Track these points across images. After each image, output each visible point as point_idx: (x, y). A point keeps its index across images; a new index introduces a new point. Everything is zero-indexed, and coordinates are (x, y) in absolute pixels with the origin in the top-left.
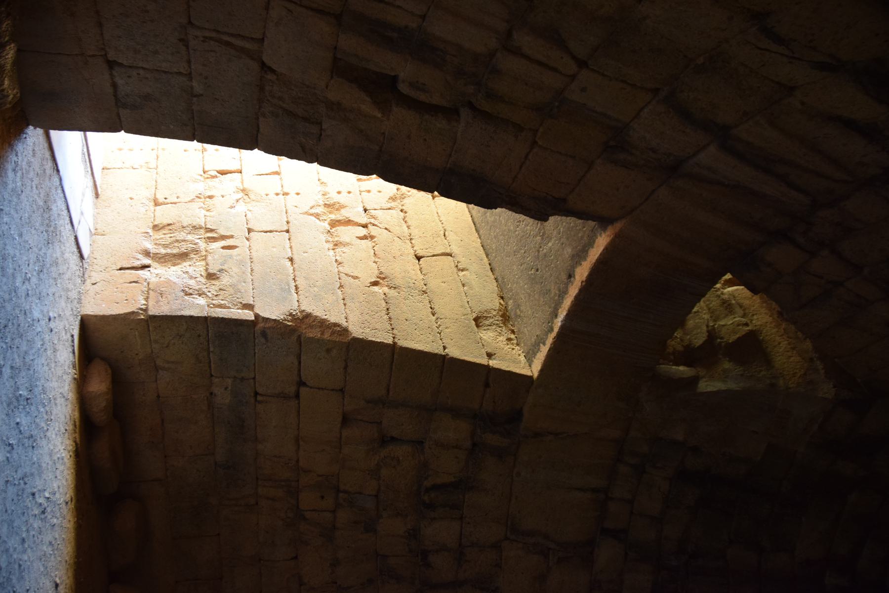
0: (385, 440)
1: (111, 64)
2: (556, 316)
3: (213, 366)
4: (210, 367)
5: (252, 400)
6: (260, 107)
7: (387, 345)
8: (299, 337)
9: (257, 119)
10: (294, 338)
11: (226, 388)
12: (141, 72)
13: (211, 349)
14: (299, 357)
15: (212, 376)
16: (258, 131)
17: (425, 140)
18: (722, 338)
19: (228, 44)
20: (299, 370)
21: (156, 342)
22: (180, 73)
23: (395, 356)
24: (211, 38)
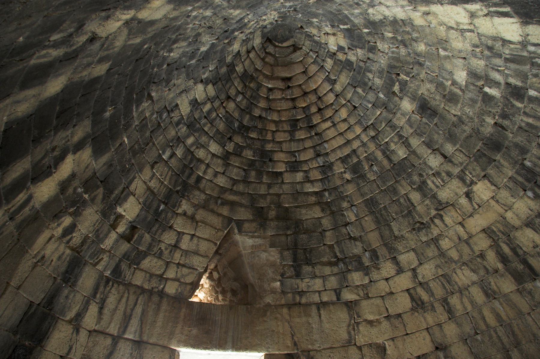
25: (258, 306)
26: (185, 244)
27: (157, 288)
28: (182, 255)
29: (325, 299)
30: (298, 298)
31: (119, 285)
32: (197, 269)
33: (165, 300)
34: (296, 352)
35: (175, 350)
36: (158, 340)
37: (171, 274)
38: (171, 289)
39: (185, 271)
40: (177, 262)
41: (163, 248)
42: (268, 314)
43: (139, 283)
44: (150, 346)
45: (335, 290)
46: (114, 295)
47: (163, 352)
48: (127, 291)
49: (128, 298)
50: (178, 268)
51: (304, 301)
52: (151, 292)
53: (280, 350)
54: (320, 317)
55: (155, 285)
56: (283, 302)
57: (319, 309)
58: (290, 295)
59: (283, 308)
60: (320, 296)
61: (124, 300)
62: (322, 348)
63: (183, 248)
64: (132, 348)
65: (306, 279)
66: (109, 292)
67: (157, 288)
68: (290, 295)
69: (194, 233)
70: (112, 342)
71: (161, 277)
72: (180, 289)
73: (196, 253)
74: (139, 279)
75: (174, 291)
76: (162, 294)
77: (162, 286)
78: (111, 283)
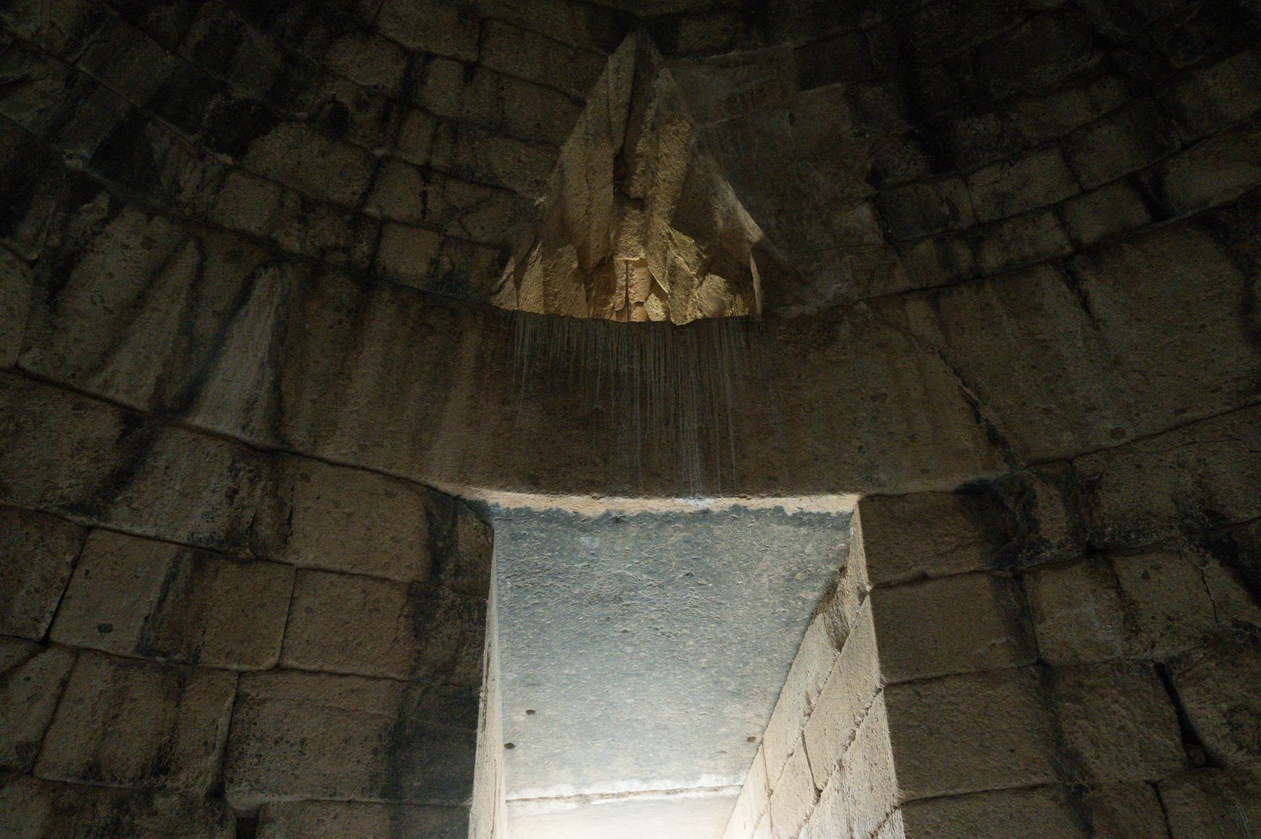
2: (706, 512)
7: (907, 820)
18: (698, 255)
23: (929, 794)
25: (795, 310)
26: (442, 91)
27: (345, 250)
28: (435, 137)
29: (1091, 229)
30: (963, 255)
31: (150, 218)
32: (512, 192)
33: (386, 295)
34: (1003, 471)
35: (457, 498)
36: (363, 448)
37: (398, 198)
38: (409, 257)
39: (460, 193)
40: (419, 159)
41: (346, 100)
42: (845, 330)
43: (254, 224)
44: (326, 469)
45: (1132, 181)
46: (126, 247)
47: (389, 494)
48: (191, 247)
49: (201, 269)
50: (426, 179)
51: (992, 258)
52: (316, 267)
53: (925, 471)
54: (1085, 305)
55: (332, 240)
56: (901, 283)
57: (1073, 280)
58: (925, 249)
59: (904, 301)
60: (1064, 225)
61: (180, 274)
62: (1131, 434)
63: (438, 113)
64: (234, 471)
65: (985, 172)
66: (94, 234)
67: (345, 250)
68: (925, 249)
69: (473, 57)
70: (124, 434)
71: (355, 217)
72: (445, 259)
73: (500, 128)
74: (248, 207)
75: (423, 268)
76: (369, 278)
77: (364, 247)
78: (103, 201)
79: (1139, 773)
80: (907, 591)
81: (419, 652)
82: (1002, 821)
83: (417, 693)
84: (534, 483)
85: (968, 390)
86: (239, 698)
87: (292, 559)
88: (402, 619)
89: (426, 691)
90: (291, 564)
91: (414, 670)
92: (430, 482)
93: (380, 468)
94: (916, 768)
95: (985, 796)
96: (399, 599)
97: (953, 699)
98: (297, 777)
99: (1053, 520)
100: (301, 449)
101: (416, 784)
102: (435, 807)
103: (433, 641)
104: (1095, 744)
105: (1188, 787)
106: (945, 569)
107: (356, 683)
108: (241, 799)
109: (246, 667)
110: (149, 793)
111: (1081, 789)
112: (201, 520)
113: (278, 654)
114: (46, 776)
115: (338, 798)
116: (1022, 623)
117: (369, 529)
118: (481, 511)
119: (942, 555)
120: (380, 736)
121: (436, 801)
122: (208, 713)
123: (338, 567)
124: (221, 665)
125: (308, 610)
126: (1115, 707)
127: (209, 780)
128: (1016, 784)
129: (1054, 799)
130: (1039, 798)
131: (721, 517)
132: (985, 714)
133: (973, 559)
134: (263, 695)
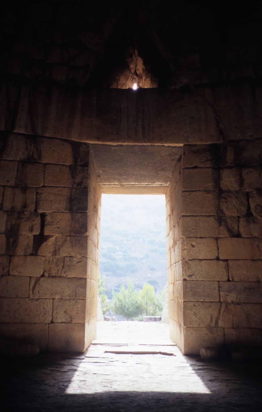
0: (249, 214)
1: (52, 322)
3: (212, 301)
4: (214, 302)
5: (232, 283)
6: (63, 277)
8: (190, 260)
9: (69, 278)
10: (190, 262)
11: (227, 295)
12: (54, 314)
13: (203, 301)
14: (201, 260)
15: (220, 301)
16: (76, 278)
17: (58, 222)
19: (34, 287)
20: (210, 260)
21: (199, 325)
22: (53, 302)
23: (188, 215)
24: (33, 292)
34: (222, 142)
35: (80, 142)
53: (201, 140)
79: (235, 215)
80: (191, 170)
81: (73, 181)
82: (203, 222)
83: (74, 190)
84: (98, 139)
85: (217, 118)
86: (37, 193)
87: (43, 162)
88: (69, 174)
89: (76, 190)
90: (42, 163)
91: (73, 185)
92: (72, 140)
93: (60, 138)
94: (187, 209)
95: (200, 216)
96: (68, 170)
97: (197, 196)
98: (51, 208)
99: (230, 157)
100: (40, 135)
101: (75, 208)
102: (80, 213)
103: (76, 178)
104: (227, 208)
105: (244, 219)
106: (202, 166)
107: (61, 189)
108: (40, 211)
109: (37, 187)
110: (23, 212)
111: (222, 217)
112: (21, 155)
113: (43, 183)
114: (5, 209)
115: (60, 211)
116: (217, 180)
117: (59, 153)
118: (86, 144)
119: (202, 162)
120: (67, 199)
121: (80, 212)
122: (32, 197)
123: (53, 163)
124: (32, 186)
125: (48, 173)
126: (233, 201)
127: (34, 208)
128: (207, 215)
129: (215, 218)
130: (212, 218)
131: (148, 146)
132: (204, 200)
133: (209, 164)
134: (41, 192)
